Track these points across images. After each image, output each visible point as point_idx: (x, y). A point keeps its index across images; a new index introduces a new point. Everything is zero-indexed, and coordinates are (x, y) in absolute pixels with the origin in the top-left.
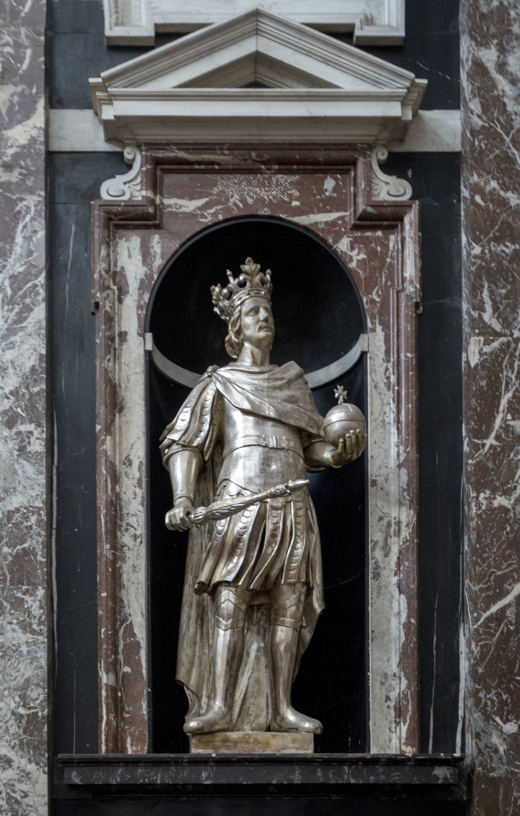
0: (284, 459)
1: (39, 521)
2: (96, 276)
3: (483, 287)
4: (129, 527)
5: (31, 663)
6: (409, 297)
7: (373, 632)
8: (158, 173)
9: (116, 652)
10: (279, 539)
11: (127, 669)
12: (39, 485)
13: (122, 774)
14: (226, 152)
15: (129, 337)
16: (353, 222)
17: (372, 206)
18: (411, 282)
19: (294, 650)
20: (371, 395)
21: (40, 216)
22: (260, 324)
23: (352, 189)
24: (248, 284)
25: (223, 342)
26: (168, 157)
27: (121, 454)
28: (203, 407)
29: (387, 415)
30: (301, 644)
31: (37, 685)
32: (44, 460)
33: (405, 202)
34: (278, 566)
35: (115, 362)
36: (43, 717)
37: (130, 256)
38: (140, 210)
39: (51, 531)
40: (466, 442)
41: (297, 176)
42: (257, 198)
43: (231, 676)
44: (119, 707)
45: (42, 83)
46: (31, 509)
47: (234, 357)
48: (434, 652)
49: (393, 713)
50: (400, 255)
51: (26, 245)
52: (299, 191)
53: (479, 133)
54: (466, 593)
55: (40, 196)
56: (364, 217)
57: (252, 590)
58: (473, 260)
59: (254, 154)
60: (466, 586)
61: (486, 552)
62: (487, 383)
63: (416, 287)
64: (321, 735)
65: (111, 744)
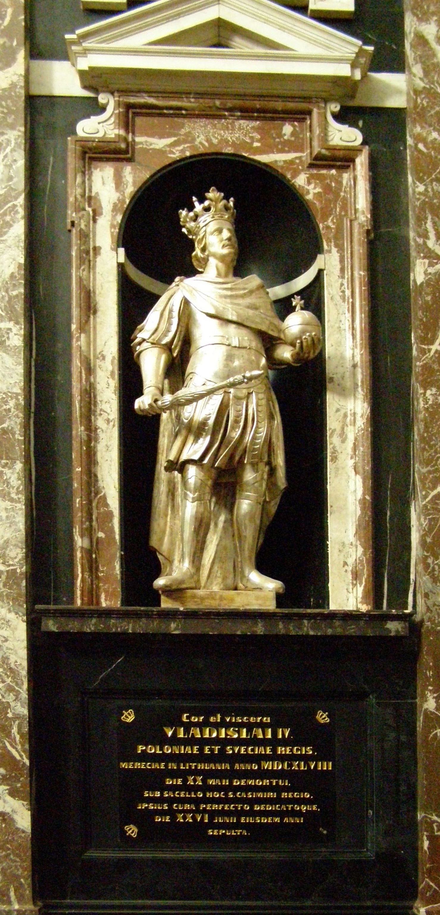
0: (246, 356)
1: (17, 406)
2: (71, 199)
3: (426, 218)
4: (102, 413)
5: (10, 526)
6: (361, 226)
7: (331, 506)
8: (130, 116)
9: (90, 520)
10: (242, 424)
11: (101, 535)
12: (17, 374)
13: (95, 624)
14: (192, 100)
15: (102, 251)
16: (309, 161)
17: (327, 149)
18: (363, 213)
19: (258, 522)
20: (328, 305)
21: (20, 148)
22: (224, 242)
23: (308, 134)
24: (212, 209)
25: (191, 258)
26: (139, 103)
27: (95, 350)
28: (171, 311)
29: (343, 322)
30: (264, 515)
31: (16, 546)
32: (22, 353)
33: (356, 146)
34: (241, 448)
35: (89, 272)
36: (21, 574)
37: (103, 183)
38: (113, 146)
39: (30, 414)
40: (414, 347)
41: (258, 122)
42: (221, 139)
43: (198, 542)
44: (94, 568)
45: (22, 38)
46: (10, 394)
47: (200, 270)
48: (388, 525)
49: (350, 577)
50: (353, 191)
51: (6, 172)
52: (259, 134)
53: (421, 92)
54: (416, 475)
55: (19, 131)
56: (318, 157)
57: (218, 468)
58: (418, 196)
59: (218, 103)
60: (416, 469)
61: (433, 440)
62: (432, 298)
63: (367, 217)
64: (285, 593)
65: (85, 599)
